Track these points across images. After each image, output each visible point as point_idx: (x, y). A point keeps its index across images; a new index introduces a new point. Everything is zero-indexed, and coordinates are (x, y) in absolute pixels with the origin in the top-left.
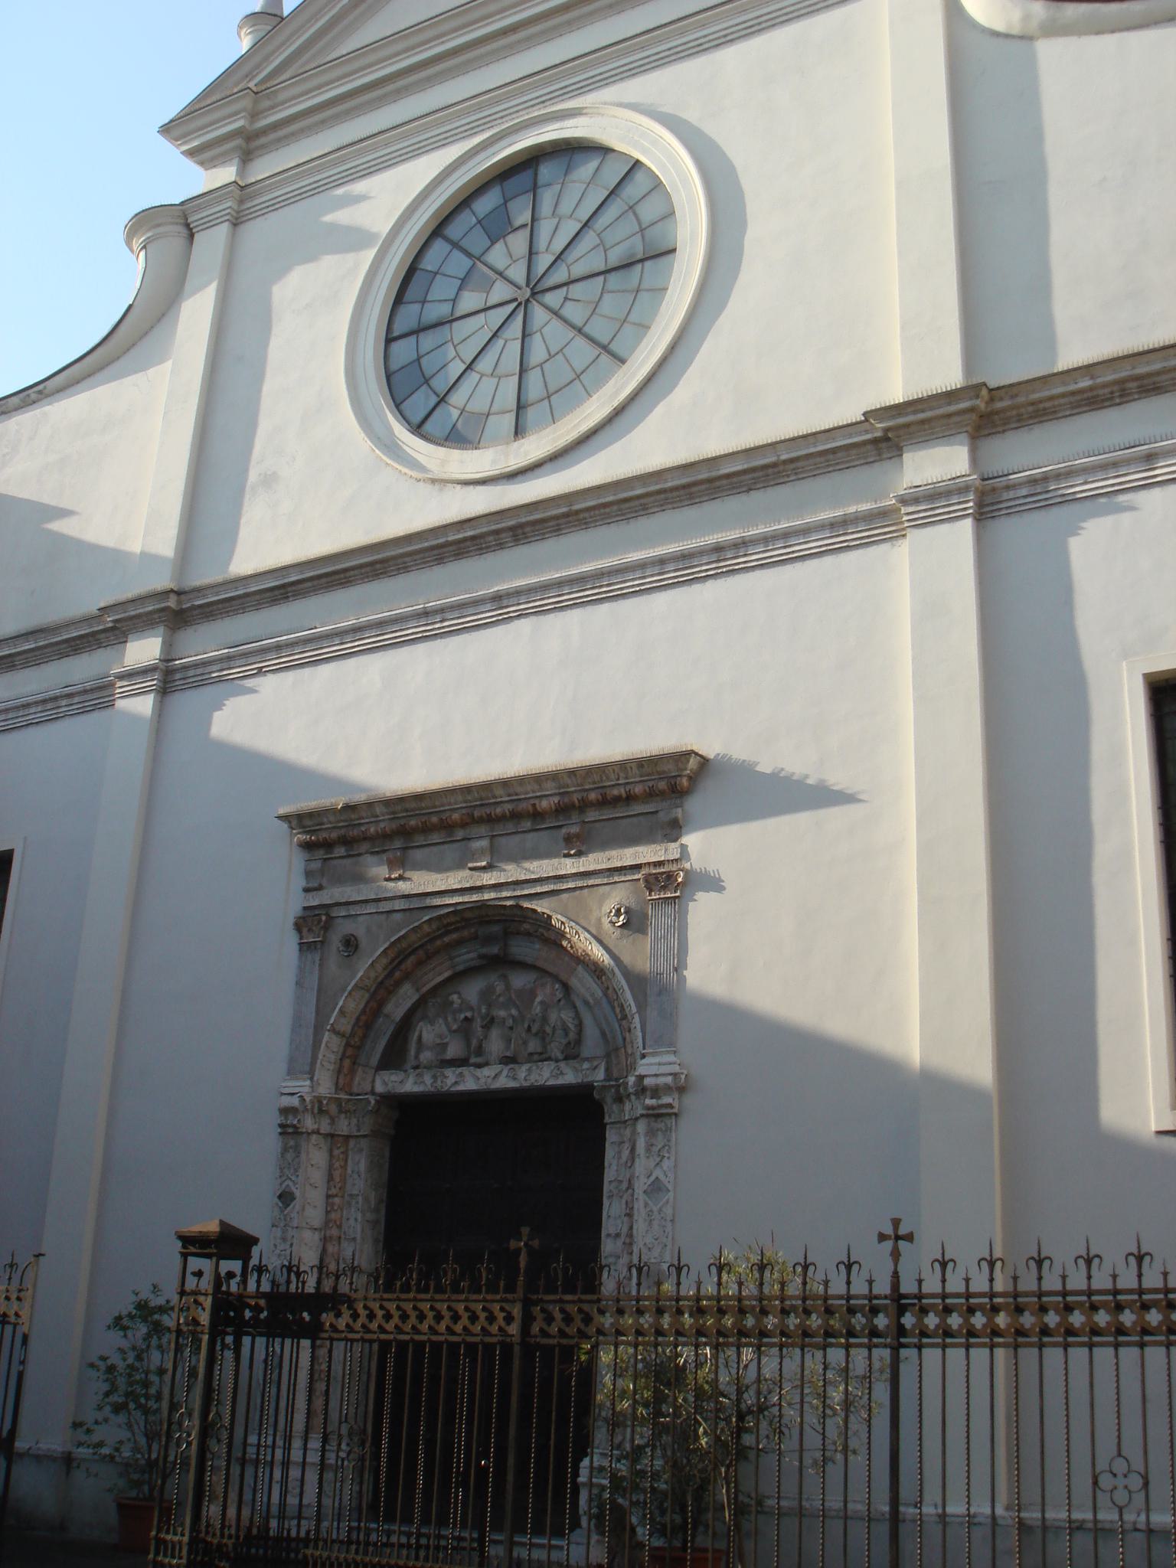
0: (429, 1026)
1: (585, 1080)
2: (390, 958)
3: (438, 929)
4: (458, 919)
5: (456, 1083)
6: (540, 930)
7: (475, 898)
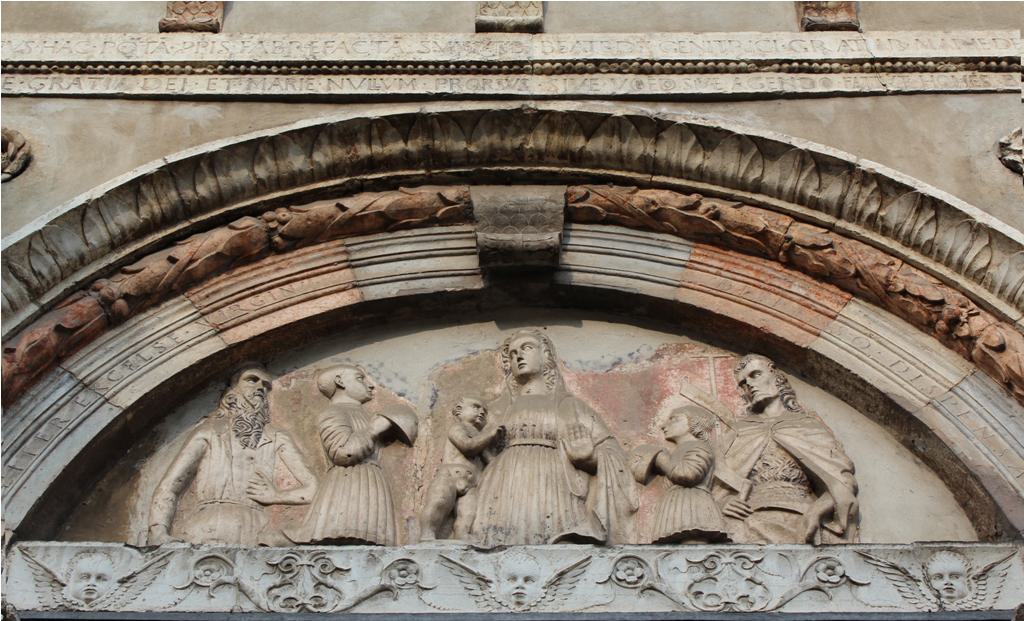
0: (236, 444)
1: (952, 607)
2: (145, 212)
3: (332, 171)
4: (413, 146)
5: (384, 589)
6: (706, 204)
7: (495, 85)
